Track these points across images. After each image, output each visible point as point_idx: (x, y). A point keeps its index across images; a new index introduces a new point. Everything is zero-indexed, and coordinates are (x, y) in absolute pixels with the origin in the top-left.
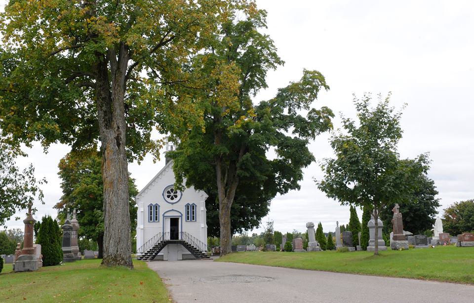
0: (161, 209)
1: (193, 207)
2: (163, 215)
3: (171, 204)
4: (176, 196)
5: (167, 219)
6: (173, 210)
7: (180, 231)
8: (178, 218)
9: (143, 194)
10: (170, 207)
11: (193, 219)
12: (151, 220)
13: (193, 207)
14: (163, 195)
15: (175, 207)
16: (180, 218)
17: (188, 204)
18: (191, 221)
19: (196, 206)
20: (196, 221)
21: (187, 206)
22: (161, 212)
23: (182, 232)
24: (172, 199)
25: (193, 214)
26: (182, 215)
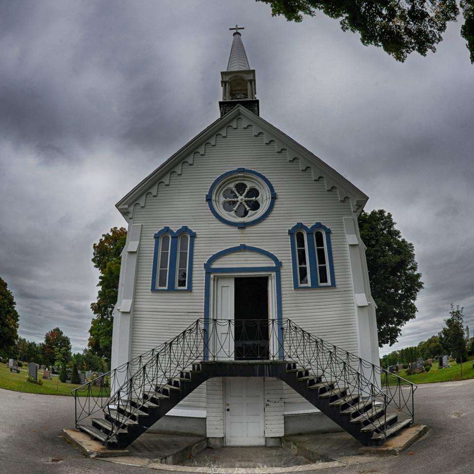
0: (199, 245)
1: (319, 234)
2: (208, 267)
3: (277, 202)
4: (254, 192)
5: (222, 283)
6: (243, 248)
7: (272, 314)
8: (265, 280)
9: (180, 166)
10: (234, 238)
11: (324, 279)
12: (162, 283)
13: (319, 234)
14: (209, 199)
15: (250, 237)
16: (274, 274)
17: (300, 226)
18: (315, 286)
19: (328, 232)
20: (334, 285)
21: (297, 234)
22: (202, 252)
23: (280, 318)
24: (255, 206)
25: (322, 260)
26: (279, 265)
